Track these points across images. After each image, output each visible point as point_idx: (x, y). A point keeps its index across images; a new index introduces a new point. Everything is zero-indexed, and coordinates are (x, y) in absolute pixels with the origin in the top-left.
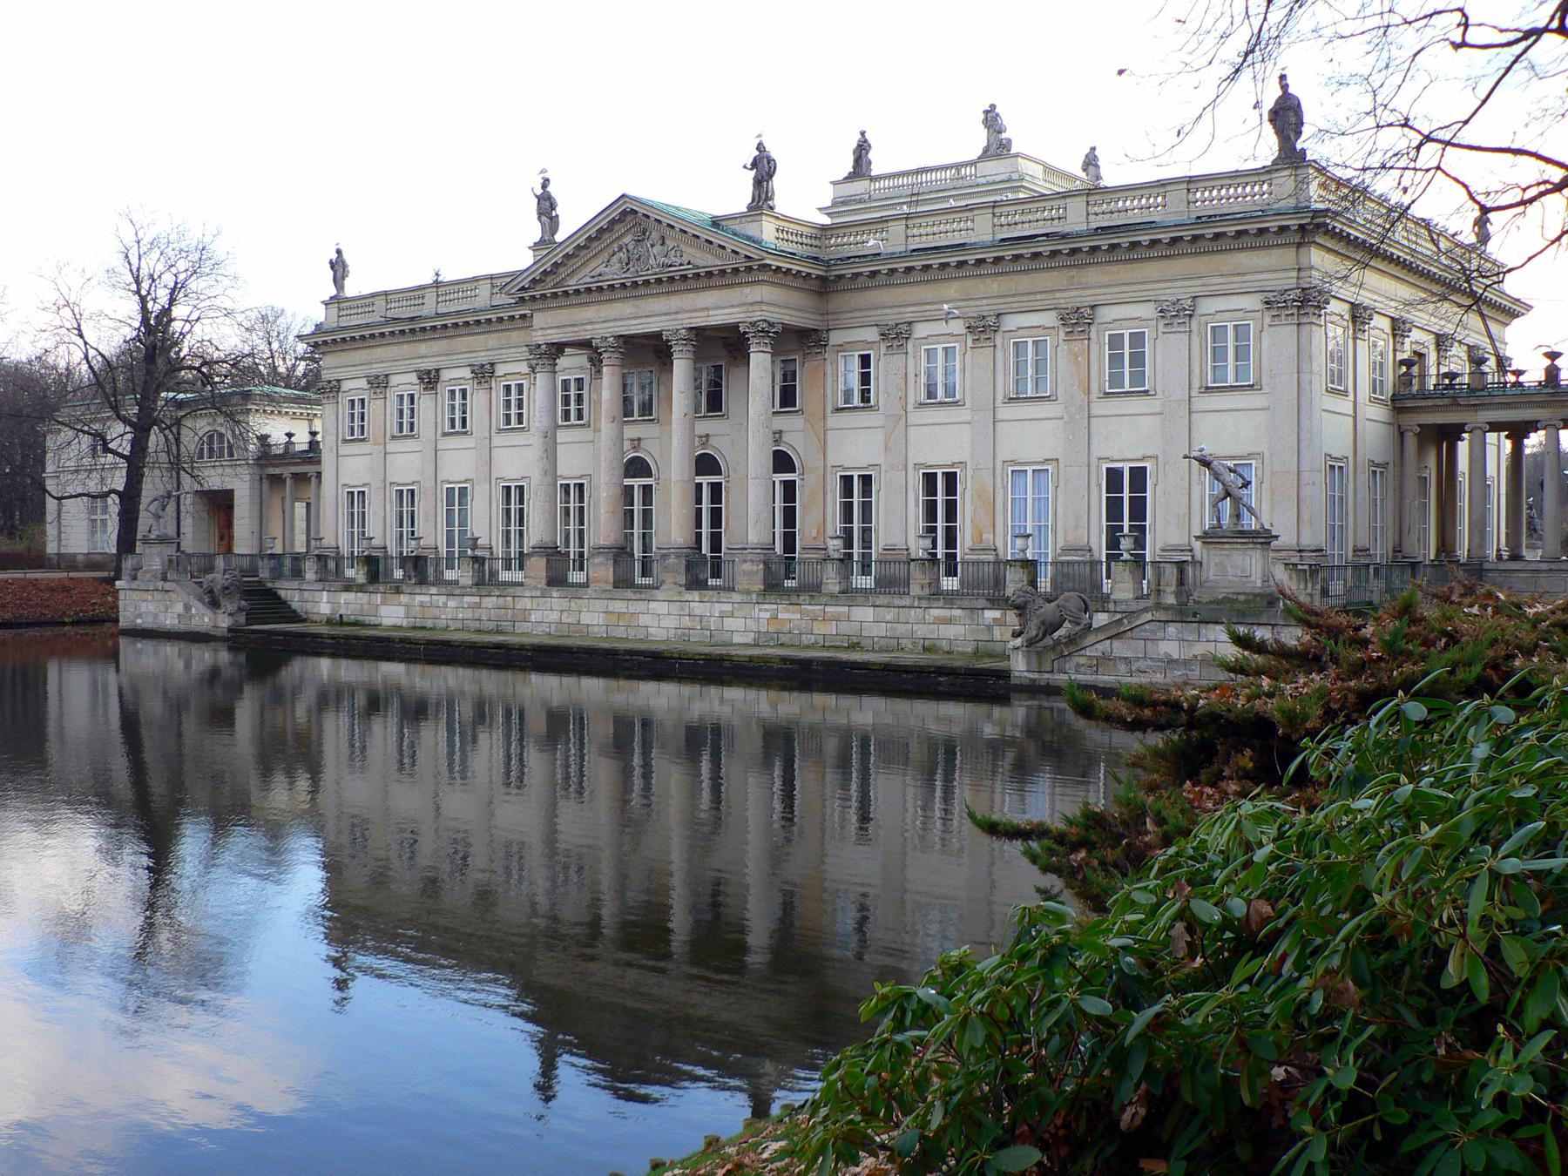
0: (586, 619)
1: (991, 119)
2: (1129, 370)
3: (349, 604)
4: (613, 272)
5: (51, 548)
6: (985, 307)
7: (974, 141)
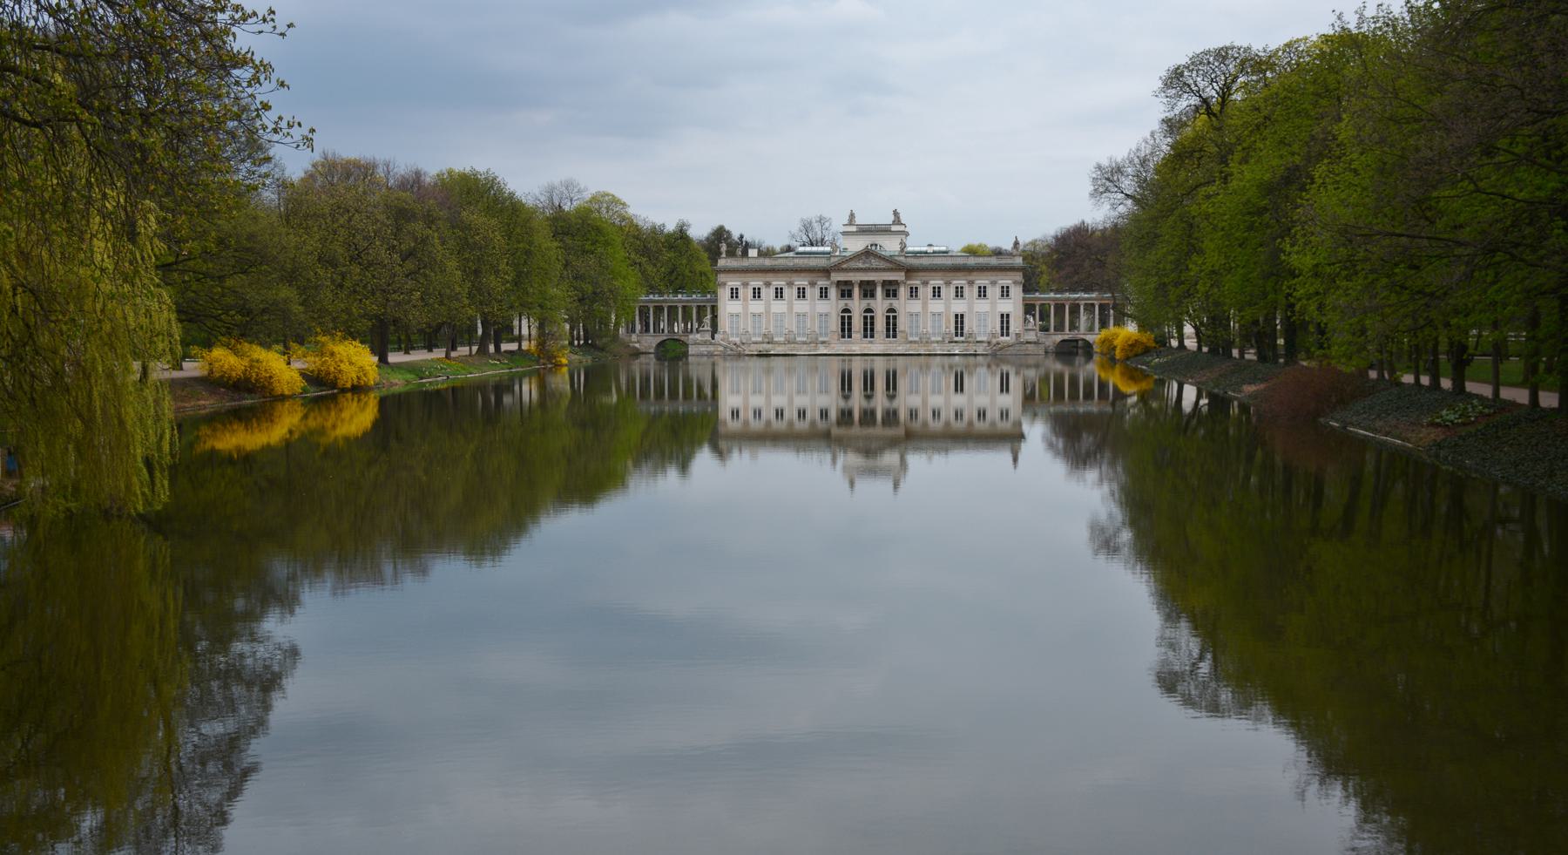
1: (896, 213)
4: (861, 265)
5: (516, 332)
7: (890, 219)
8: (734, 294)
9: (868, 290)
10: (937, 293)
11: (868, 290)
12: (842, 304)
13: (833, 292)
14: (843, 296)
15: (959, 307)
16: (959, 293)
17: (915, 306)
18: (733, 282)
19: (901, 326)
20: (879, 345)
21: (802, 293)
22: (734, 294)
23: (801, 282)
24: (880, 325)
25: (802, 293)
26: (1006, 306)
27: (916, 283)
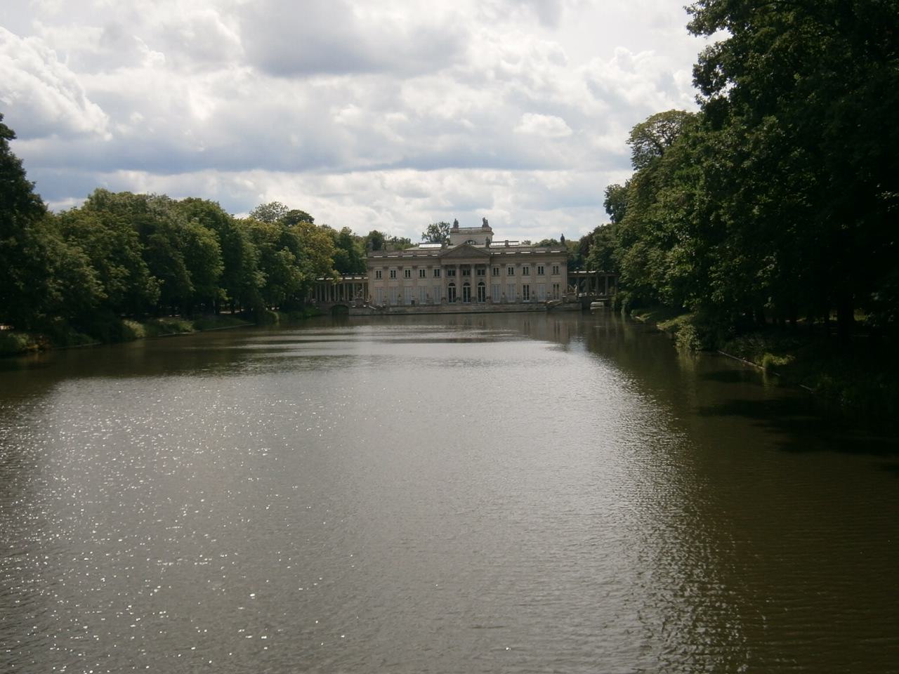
0: (458, 309)
1: (484, 220)
2: (541, 271)
3: (396, 309)
6: (519, 262)
8: (379, 275)
9: (466, 271)
10: (511, 271)
11: (466, 271)
12: (449, 280)
13: (443, 273)
14: (449, 274)
15: (526, 280)
16: (525, 272)
17: (497, 281)
18: (379, 268)
19: (488, 294)
20: (472, 308)
21: (422, 274)
22: (379, 275)
23: (423, 266)
24: (474, 293)
25: (422, 274)
26: (557, 279)
27: (497, 265)
